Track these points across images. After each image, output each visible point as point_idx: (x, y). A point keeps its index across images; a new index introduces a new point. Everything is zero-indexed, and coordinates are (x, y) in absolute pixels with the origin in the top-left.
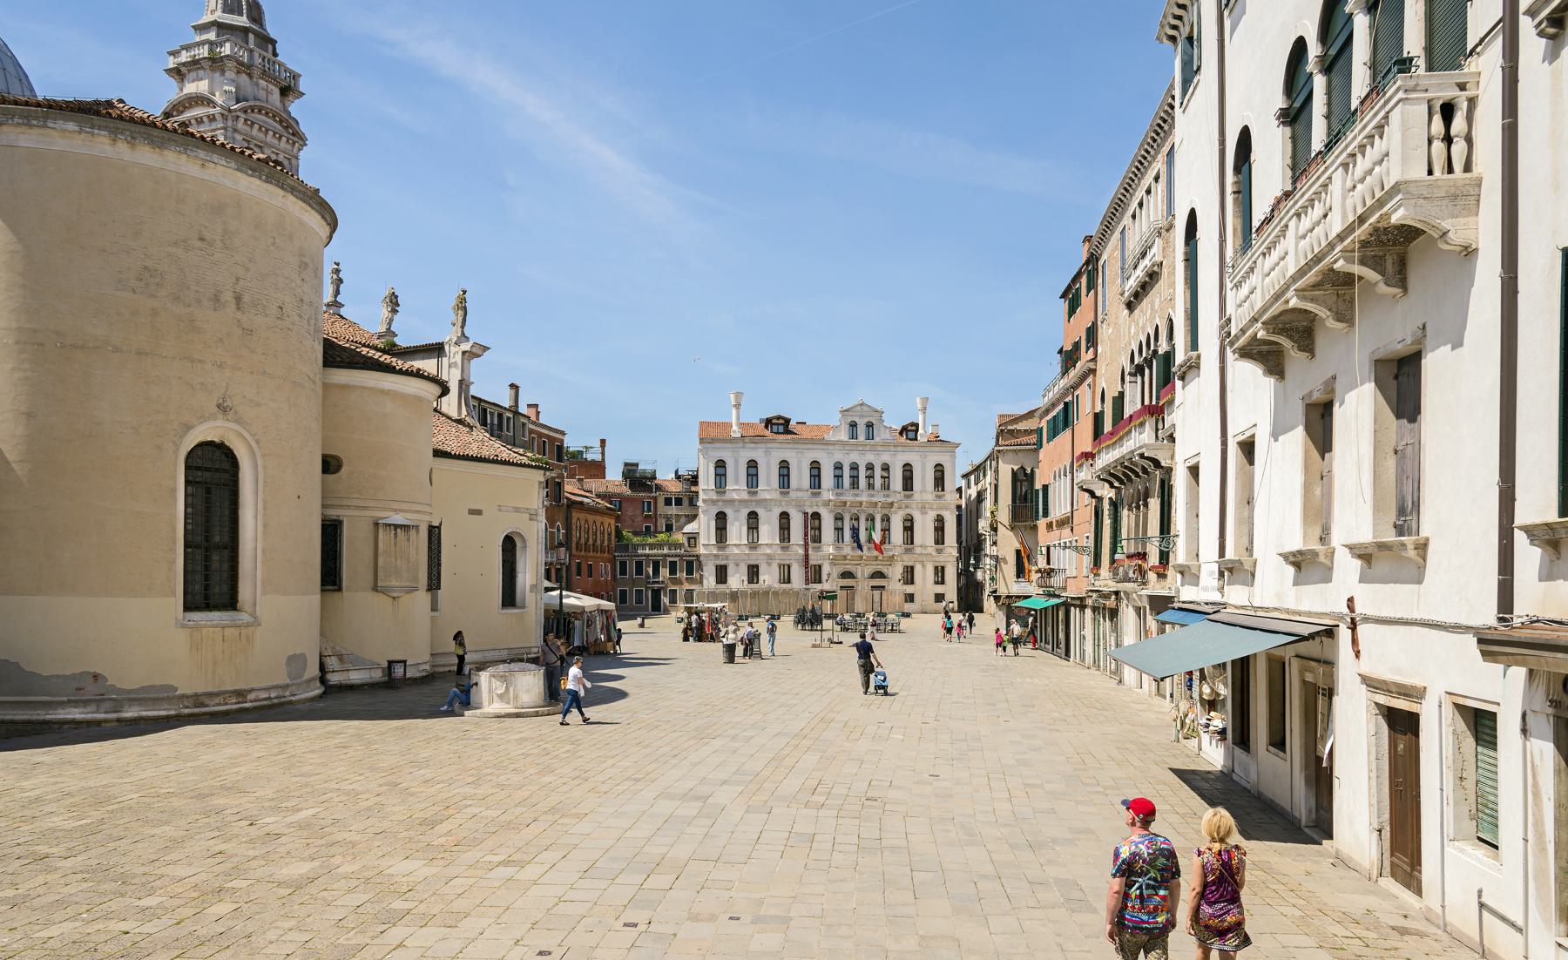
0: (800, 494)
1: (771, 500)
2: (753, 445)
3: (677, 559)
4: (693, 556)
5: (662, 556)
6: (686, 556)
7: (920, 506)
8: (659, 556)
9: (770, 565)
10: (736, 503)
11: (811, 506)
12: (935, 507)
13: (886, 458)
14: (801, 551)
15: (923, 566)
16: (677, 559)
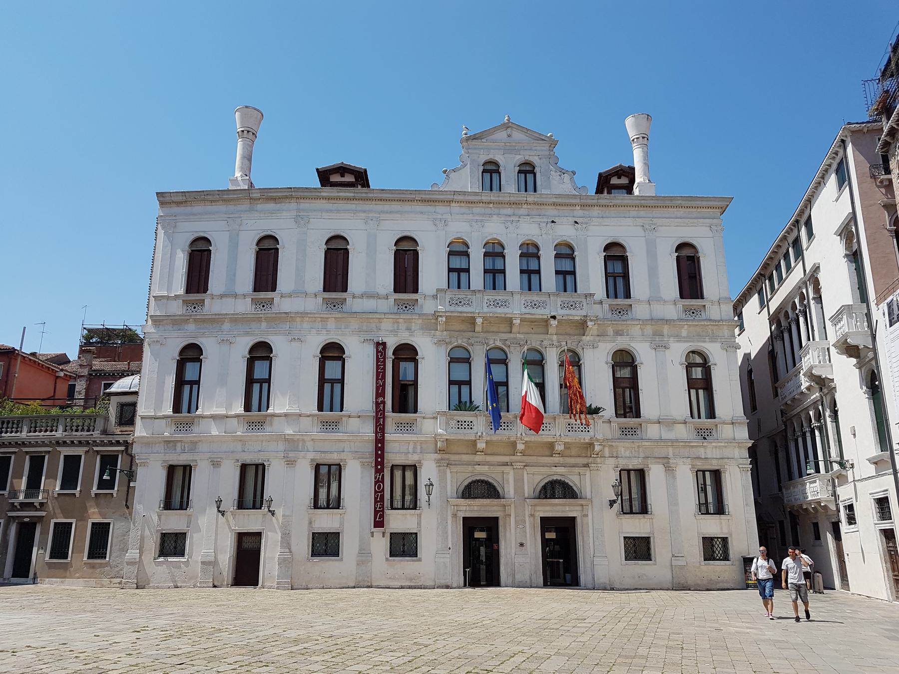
0: (369, 304)
1: (303, 315)
2: (271, 206)
3: (80, 451)
4: (118, 443)
5: (50, 444)
6: (102, 444)
7: (649, 330)
8: (44, 444)
9: (291, 463)
10: (226, 326)
11: (395, 332)
12: (684, 333)
13: (565, 231)
14: (368, 431)
15: (669, 469)
16: (80, 451)
